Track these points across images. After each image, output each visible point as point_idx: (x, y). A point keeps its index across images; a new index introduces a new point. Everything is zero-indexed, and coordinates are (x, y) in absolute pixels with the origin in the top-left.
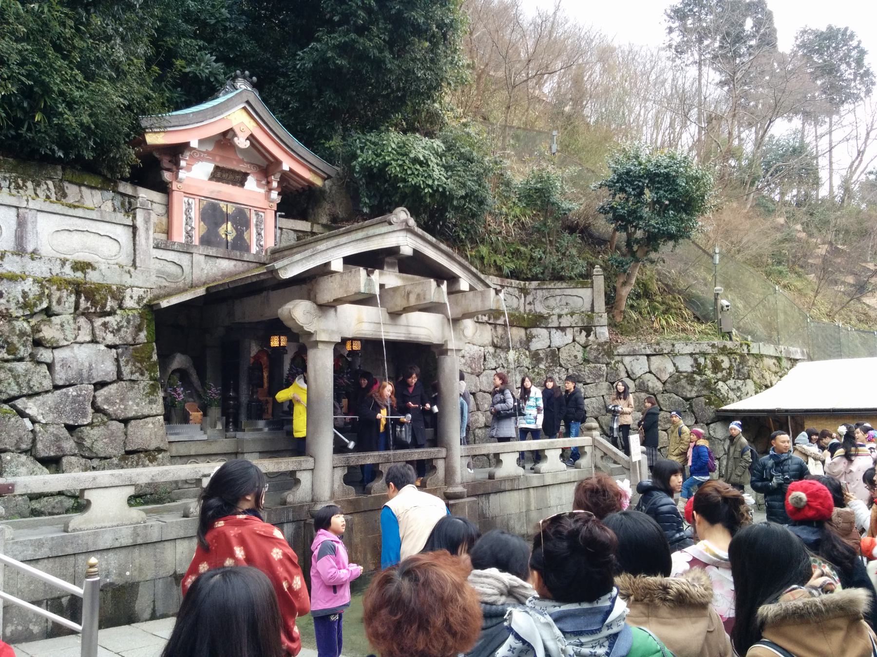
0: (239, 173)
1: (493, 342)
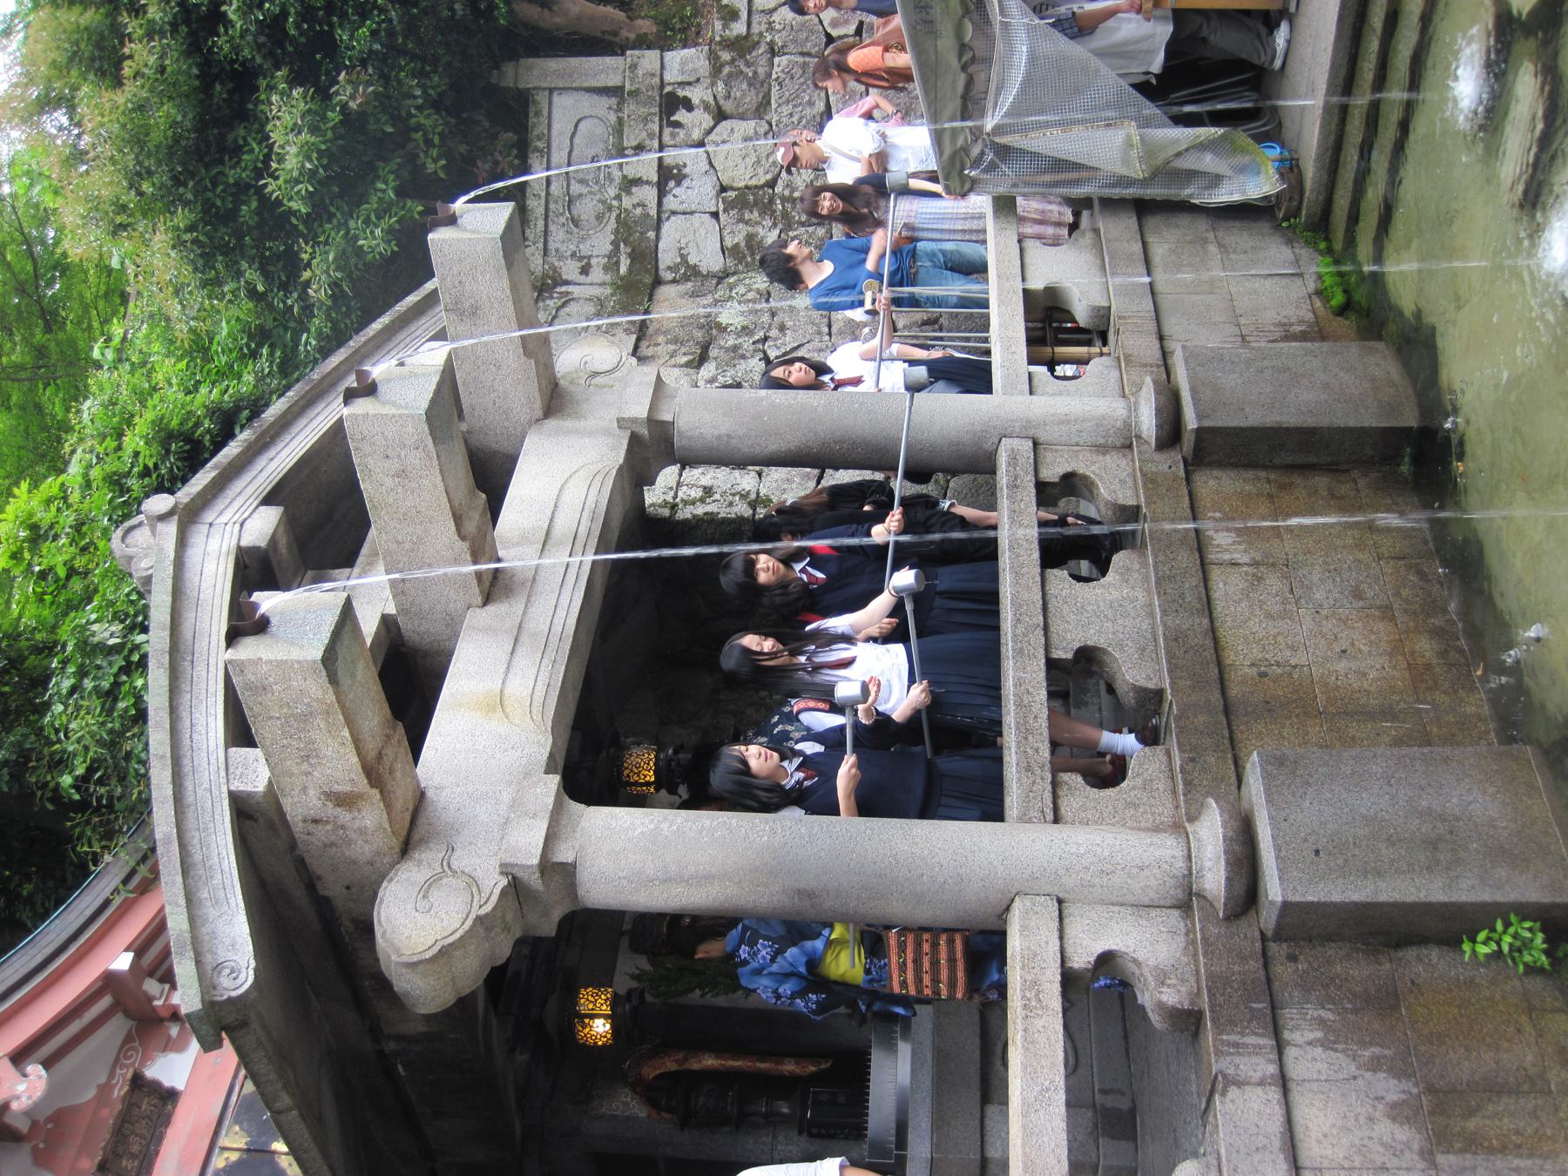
0: (130, 1103)
1: (688, 365)
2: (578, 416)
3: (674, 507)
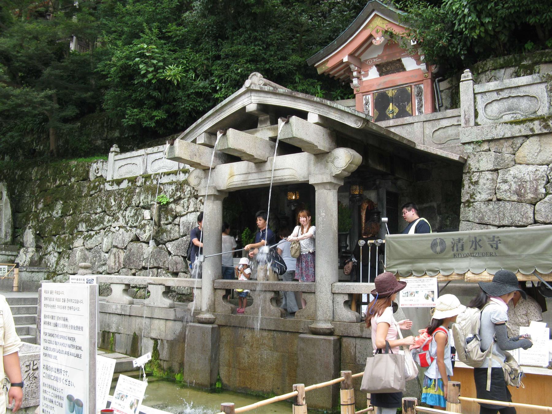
2: (314, 164)
3: (469, 172)
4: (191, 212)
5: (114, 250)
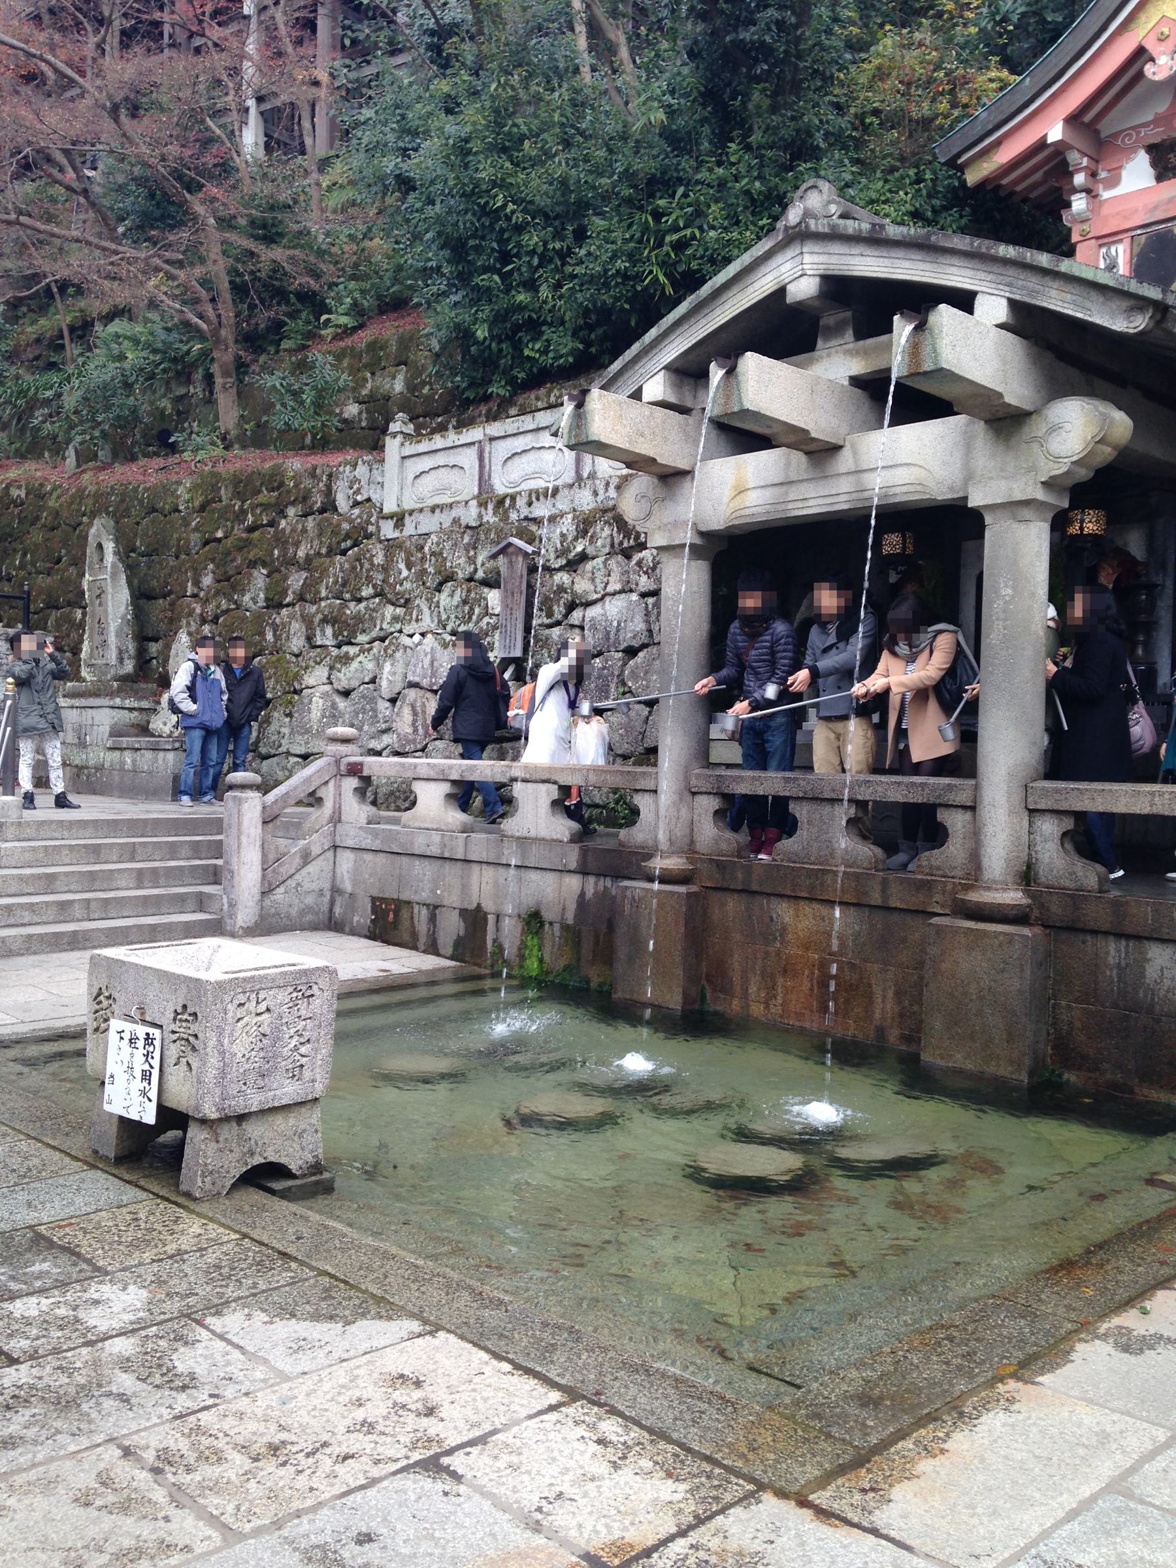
4: (614, 594)
5: (412, 694)
